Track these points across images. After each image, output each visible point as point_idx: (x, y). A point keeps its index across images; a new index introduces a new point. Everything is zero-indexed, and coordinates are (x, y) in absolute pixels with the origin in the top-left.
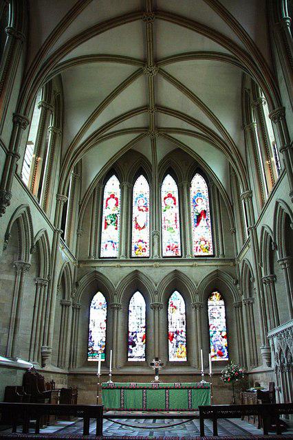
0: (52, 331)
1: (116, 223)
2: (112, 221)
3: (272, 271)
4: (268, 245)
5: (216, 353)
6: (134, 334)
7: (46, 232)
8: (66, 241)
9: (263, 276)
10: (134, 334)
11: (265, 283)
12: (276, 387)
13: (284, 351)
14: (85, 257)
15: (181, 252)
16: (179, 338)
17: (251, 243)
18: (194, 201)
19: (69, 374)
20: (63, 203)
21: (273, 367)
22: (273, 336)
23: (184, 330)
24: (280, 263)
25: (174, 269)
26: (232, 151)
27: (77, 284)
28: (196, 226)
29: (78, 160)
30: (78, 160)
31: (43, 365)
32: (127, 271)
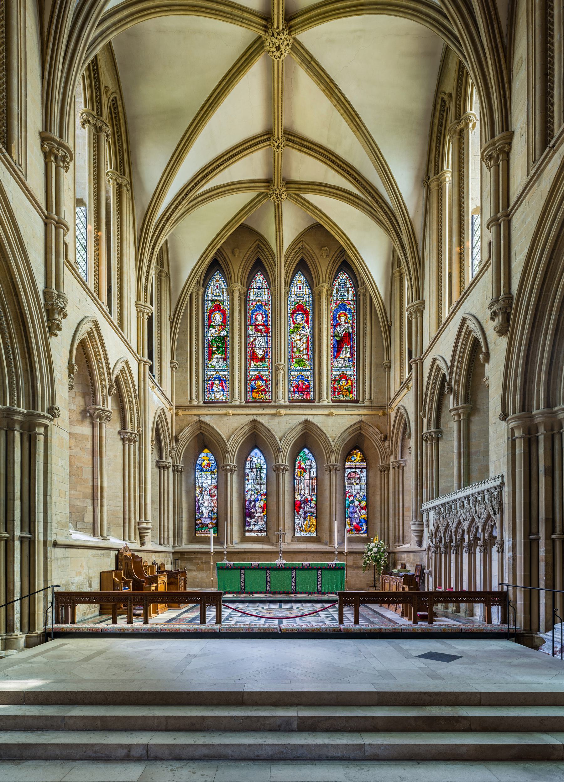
0: (149, 501)
1: (225, 350)
2: (218, 348)
3: (438, 425)
4: (438, 386)
5: (352, 527)
6: (253, 503)
7: (126, 362)
8: (157, 376)
9: (425, 430)
10: (253, 503)
11: (426, 441)
12: (426, 571)
13: (442, 529)
14: (184, 401)
15: (314, 395)
16: (308, 509)
17: (412, 384)
18: (334, 318)
19: (174, 553)
20: (146, 317)
21: (425, 546)
22: (427, 510)
23: (313, 498)
24: (453, 413)
25: (303, 418)
26: (403, 228)
27: (176, 439)
28: (336, 357)
29: (161, 242)
30: (161, 242)
31: (142, 544)
32: (246, 420)
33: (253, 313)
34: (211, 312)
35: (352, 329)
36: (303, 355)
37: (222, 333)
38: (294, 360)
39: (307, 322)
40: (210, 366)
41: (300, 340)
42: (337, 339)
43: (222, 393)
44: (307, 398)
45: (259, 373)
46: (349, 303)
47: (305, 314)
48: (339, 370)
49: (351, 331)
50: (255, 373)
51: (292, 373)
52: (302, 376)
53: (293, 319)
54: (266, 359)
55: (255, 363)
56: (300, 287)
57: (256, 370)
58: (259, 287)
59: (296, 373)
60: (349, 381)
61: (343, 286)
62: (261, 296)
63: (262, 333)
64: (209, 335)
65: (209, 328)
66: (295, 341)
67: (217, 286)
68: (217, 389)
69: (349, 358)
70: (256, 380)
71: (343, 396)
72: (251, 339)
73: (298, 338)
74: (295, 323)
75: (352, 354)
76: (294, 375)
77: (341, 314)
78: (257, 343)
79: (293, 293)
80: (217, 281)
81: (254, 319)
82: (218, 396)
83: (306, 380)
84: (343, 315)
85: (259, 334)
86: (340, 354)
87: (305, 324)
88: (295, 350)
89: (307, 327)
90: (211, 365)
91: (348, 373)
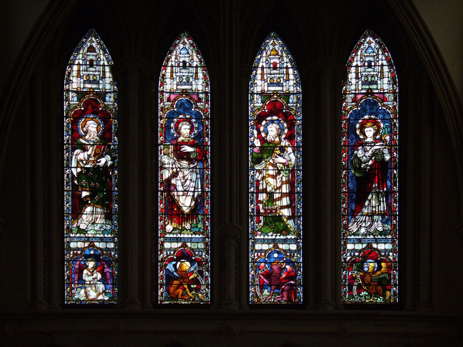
2: (94, 192)
28: (353, 214)
33: (170, 118)
34: (78, 116)
35: (391, 153)
36: (282, 207)
37: (103, 161)
38: (261, 218)
39: (290, 137)
40: (75, 230)
41: (274, 177)
42: (357, 175)
43: (101, 287)
44: (289, 299)
45: (184, 245)
46: (384, 100)
47: (286, 121)
48: (360, 241)
49: (387, 157)
50: (175, 245)
51: (258, 247)
52: (278, 253)
53: (259, 133)
54: (200, 217)
55: (175, 225)
56: (275, 64)
57: (177, 240)
58: (184, 62)
59: (265, 247)
60: (383, 264)
61: (370, 62)
62: (188, 83)
63: (191, 161)
64: (74, 164)
65: (73, 150)
66: (263, 178)
67: (91, 61)
68: (91, 278)
69: (382, 215)
70: (177, 260)
71: (370, 295)
72: (166, 174)
73: (271, 172)
74: (263, 140)
75: (389, 206)
76: (261, 251)
77: (367, 121)
78: (179, 183)
79: (259, 77)
80: (91, 49)
81: (172, 131)
82: (93, 295)
83: (288, 262)
84: (369, 124)
85: (185, 163)
86: (363, 206)
87: (285, 143)
88: (263, 197)
89: (290, 150)
90: (78, 227)
91: (381, 247)
